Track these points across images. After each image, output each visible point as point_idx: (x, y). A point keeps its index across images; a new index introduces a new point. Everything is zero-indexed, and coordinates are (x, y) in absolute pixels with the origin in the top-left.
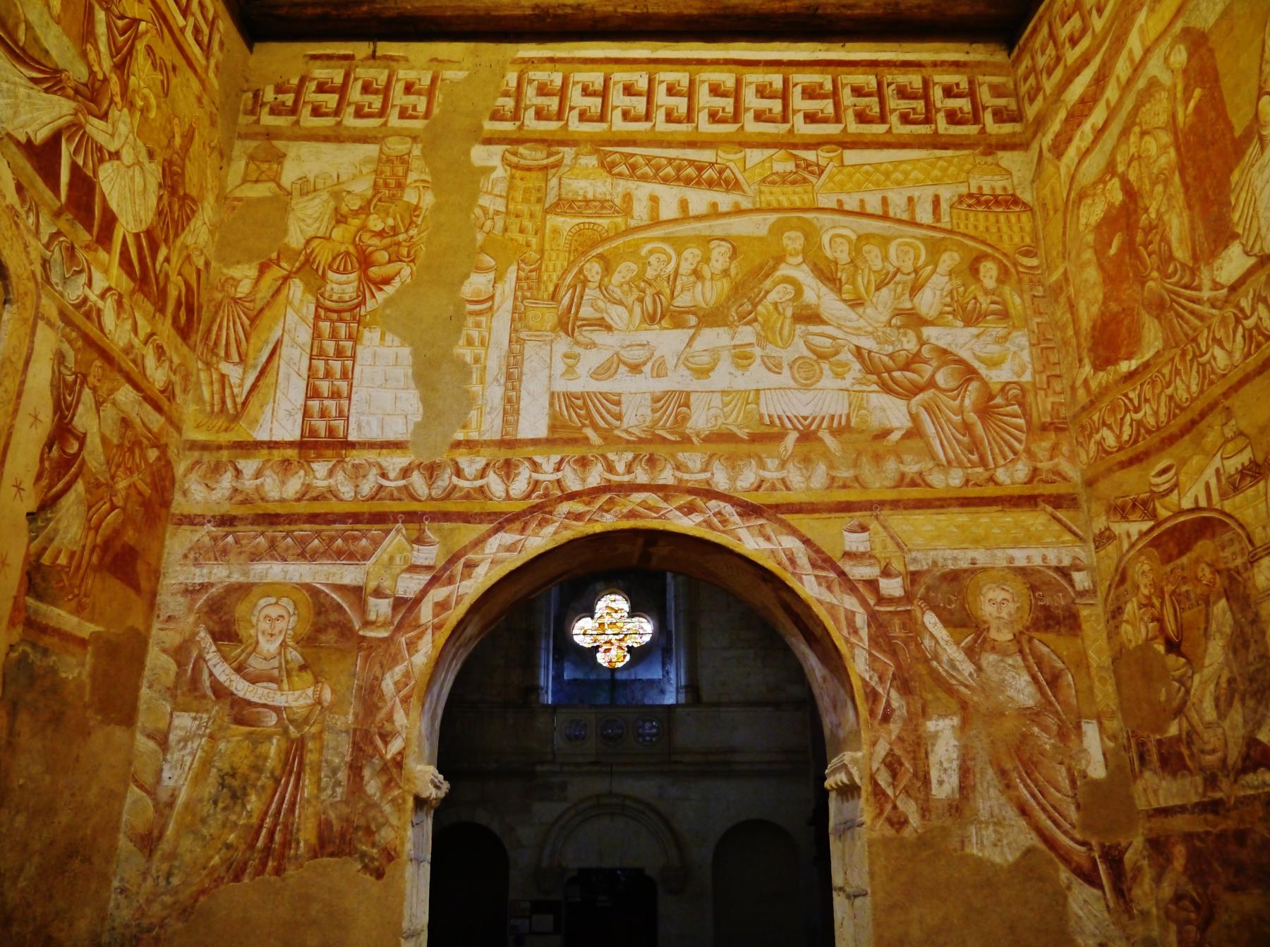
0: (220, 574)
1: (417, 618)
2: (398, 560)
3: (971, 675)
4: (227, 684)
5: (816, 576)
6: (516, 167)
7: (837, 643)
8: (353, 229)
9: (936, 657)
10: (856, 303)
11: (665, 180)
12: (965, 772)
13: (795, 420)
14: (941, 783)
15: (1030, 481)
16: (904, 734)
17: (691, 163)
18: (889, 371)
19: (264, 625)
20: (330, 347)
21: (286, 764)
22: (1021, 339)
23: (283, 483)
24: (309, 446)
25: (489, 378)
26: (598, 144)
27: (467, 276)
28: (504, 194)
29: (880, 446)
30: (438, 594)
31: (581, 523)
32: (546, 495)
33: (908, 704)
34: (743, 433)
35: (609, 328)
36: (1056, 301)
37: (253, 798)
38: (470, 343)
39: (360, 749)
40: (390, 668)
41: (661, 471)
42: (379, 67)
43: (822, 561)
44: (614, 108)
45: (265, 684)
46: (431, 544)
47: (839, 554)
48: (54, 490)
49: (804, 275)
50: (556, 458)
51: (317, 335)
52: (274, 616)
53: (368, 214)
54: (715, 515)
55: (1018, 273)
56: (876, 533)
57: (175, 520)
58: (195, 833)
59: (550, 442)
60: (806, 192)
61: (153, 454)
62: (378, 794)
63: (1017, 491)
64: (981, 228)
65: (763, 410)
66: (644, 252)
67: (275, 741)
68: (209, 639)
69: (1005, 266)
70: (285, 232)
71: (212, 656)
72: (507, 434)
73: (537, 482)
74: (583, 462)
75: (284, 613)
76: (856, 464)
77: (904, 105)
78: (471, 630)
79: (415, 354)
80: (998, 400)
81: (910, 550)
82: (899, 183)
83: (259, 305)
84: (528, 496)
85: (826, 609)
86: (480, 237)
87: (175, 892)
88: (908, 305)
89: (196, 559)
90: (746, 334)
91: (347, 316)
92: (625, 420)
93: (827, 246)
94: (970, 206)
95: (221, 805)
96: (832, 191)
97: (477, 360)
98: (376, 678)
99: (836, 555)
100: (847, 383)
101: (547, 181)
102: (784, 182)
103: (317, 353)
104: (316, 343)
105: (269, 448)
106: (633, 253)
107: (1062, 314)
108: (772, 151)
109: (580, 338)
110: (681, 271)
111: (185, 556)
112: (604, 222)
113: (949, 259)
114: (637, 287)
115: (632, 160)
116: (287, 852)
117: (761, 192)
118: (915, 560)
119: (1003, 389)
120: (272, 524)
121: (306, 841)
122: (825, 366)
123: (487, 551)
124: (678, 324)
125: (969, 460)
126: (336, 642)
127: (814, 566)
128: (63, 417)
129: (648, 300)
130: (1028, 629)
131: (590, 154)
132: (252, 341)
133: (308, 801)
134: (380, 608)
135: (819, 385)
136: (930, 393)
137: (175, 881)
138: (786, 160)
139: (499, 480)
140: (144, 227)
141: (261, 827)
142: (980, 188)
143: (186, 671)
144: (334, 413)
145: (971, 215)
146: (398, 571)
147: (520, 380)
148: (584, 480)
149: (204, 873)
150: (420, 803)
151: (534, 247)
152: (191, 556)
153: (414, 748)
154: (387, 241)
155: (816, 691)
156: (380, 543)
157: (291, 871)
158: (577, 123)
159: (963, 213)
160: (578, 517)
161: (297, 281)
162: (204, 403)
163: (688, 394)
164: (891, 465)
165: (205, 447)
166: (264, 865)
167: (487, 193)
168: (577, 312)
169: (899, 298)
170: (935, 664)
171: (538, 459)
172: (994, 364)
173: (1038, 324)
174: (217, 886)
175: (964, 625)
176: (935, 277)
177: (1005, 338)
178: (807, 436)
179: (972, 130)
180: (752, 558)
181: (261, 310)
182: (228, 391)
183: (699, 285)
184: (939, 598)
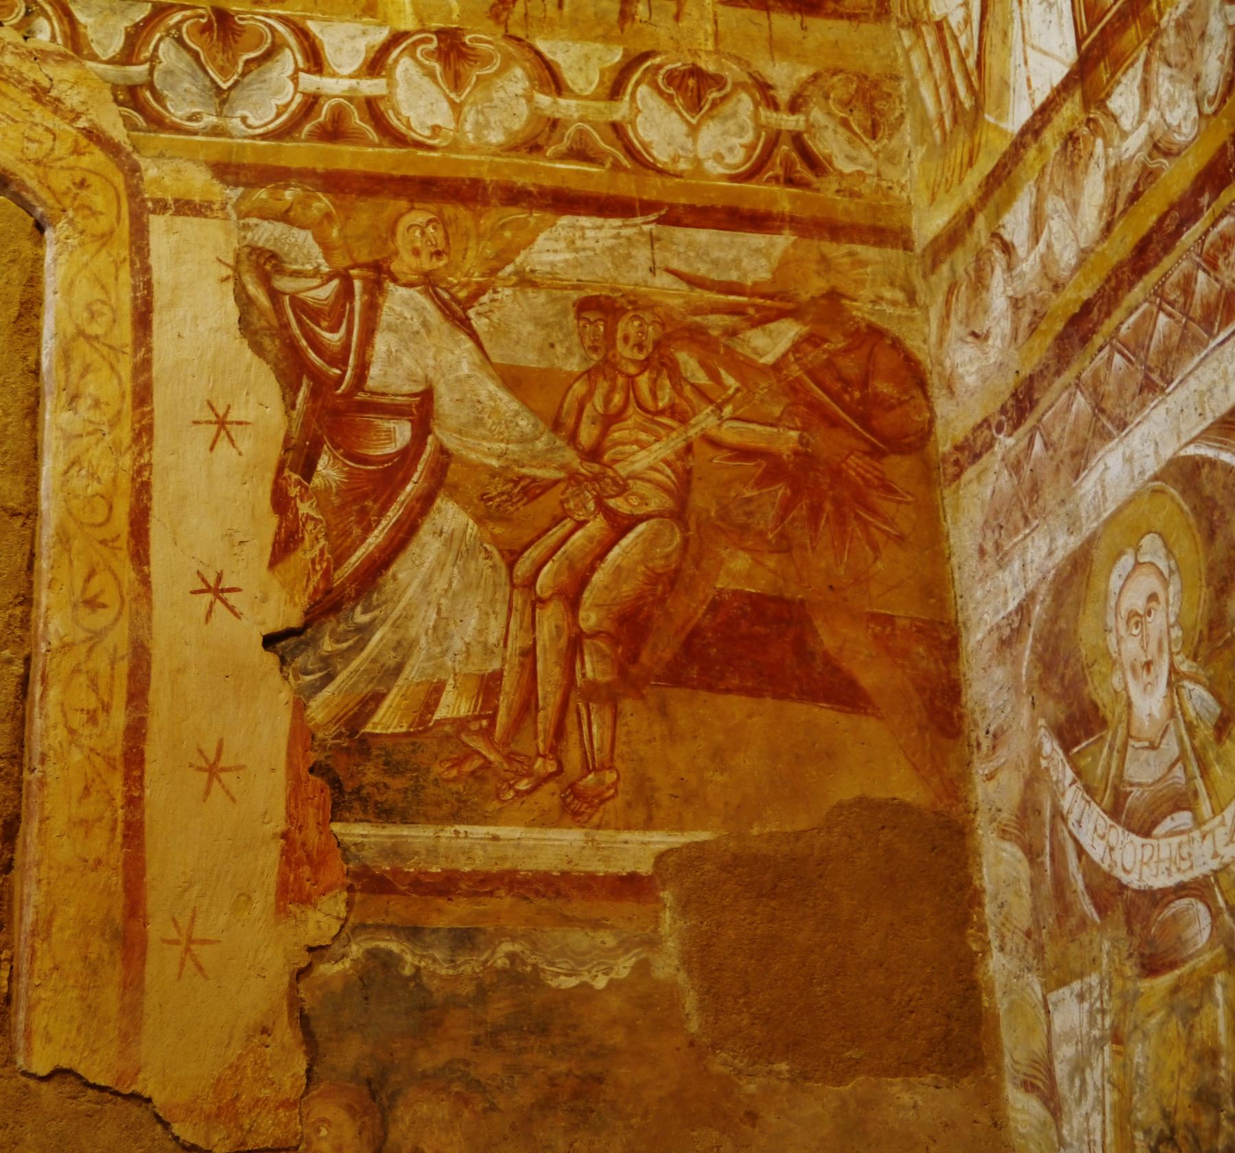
48: (356, 558)
52: (1140, 605)
61: (773, 342)
128: (321, 386)
143: (1043, 863)
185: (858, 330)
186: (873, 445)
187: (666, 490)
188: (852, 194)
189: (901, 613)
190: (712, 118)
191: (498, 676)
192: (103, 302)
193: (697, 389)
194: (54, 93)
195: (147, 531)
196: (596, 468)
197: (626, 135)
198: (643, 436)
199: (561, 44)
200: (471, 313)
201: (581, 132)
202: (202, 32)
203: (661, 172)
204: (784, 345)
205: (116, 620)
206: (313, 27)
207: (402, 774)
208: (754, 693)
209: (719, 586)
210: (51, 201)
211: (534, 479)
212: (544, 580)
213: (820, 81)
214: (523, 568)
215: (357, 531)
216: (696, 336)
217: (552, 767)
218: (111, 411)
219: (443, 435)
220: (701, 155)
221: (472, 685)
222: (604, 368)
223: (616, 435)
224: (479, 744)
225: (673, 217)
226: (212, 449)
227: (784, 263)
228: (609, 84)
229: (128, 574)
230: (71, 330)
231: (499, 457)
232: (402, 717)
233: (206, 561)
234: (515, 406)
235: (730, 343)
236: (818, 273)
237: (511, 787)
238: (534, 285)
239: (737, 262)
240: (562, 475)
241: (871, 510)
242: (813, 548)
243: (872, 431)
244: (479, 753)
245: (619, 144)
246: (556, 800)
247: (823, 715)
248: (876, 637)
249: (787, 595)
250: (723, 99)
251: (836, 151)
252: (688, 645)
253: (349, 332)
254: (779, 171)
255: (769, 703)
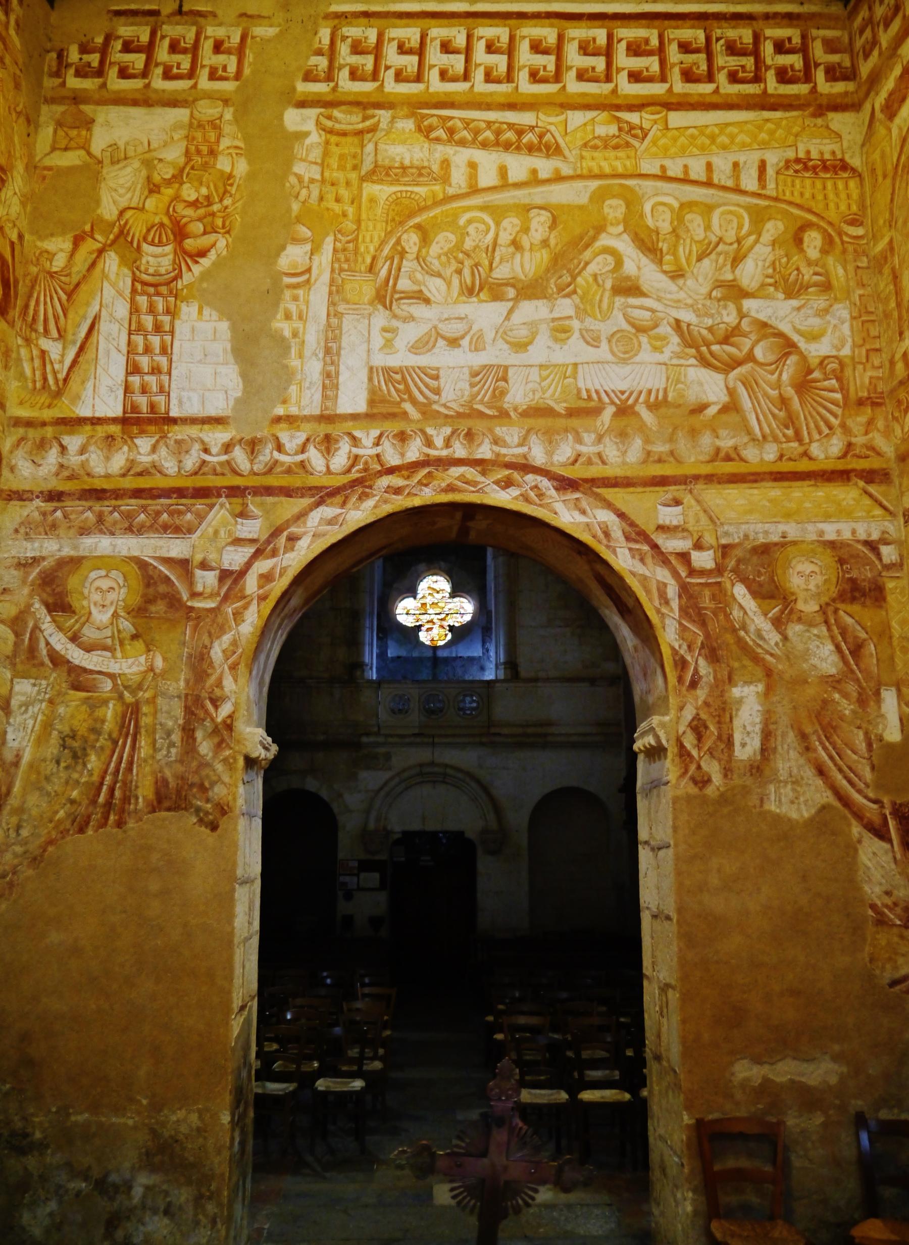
0: (51, 548)
1: (243, 589)
2: (222, 533)
3: (777, 644)
4: (63, 653)
5: (630, 549)
6: (331, 132)
7: (649, 613)
8: (166, 199)
9: (744, 627)
10: (677, 275)
11: (484, 145)
12: (767, 735)
13: (612, 395)
14: (744, 745)
15: (844, 456)
16: (710, 700)
17: (511, 126)
18: (708, 345)
19: (96, 597)
20: (148, 321)
21: (122, 726)
22: (842, 311)
23: (108, 459)
24: (131, 422)
25: (307, 353)
26: (415, 106)
27: (283, 248)
28: (319, 161)
29: (697, 420)
30: (263, 566)
31: (400, 497)
32: (365, 470)
33: (715, 671)
34: (560, 408)
35: (427, 301)
36: (880, 272)
37: (93, 758)
38: (288, 317)
39: (193, 713)
40: (218, 638)
41: (479, 445)
42: (186, 23)
43: (637, 534)
44: (431, 67)
45: (99, 652)
46: (254, 518)
47: (653, 528)
49: (625, 246)
50: (375, 433)
51: (134, 309)
52: (105, 587)
53: (182, 183)
54: (531, 489)
55: (843, 242)
56: (692, 507)
57: (4, 496)
58: (40, 789)
59: (369, 417)
60: (628, 157)
62: (211, 754)
63: (830, 465)
64: (807, 195)
65: (581, 385)
66: (462, 221)
67: (111, 705)
68: (44, 611)
69: (830, 236)
70: (98, 202)
71: (47, 625)
72: (326, 409)
73: (356, 457)
74: (402, 437)
75: (115, 586)
76: (671, 440)
77: (733, 62)
78: (295, 602)
79: (234, 328)
80: (816, 375)
81: (722, 524)
82: (724, 148)
83: (75, 279)
84: (349, 471)
85: (639, 581)
86: (295, 207)
87: (25, 843)
88: (730, 277)
89: (27, 534)
90: (565, 307)
91: (164, 290)
92: (443, 394)
93: (649, 215)
94: (796, 171)
95: (63, 765)
96: (655, 156)
97: (295, 335)
98: (206, 647)
99: (650, 528)
100: (665, 357)
101: (362, 146)
102: (606, 147)
103: (135, 329)
104: (134, 318)
105: (93, 424)
106: (452, 223)
107: (884, 285)
108: (594, 114)
109: (397, 311)
110: (500, 241)
111: (17, 531)
112: (422, 190)
113: (773, 229)
114: (455, 258)
115: (450, 124)
116: (127, 806)
117: (582, 158)
118: (726, 534)
119: (821, 363)
120: (99, 499)
121: (144, 797)
122: (644, 339)
123: (310, 523)
124: (497, 297)
125: (784, 435)
126: (165, 612)
127: (628, 539)
129: (467, 272)
130: (834, 600)
131: (407, 117)
132: (71, 315)
133: (145, 761)
134: (207, 580)
135: (637, 359)
136: (748, 366)
137: (25, 833)
138: (609, 123)
139: (319, 455)
141: (102, 784)
142: (808, 152)
143: (23, 640)
144: (154, 389)
145: (798, 182)
146: (223, 544)
147: (338, 354)
148: (403, 455)
149: (51, 825)
150: (250, 762)
151: (351, 216)
152: (22, 530)
153: (243, 712)
154: (201, 212)
155: (628, 660)
156: (205, 517)
157: (131, 824)
158: (393, 83)
159: (789, 179)
160: (398, 491)
161: (112, 254)
162: (26, 379)
163: (506, 368)
164: (706, 441)
165: (29, 423)
166: (106, 818)
167: (301, 160)
168: (395, 284)
169: (720, 269)
170: (742, 633)
171: (357, 434)
172: (814, 337)
173: (860, 296)
174: (63, 838)
175: (772, 597)
176: (758, 247)
177: (826, 311)
178: (624, 411)
179: (802, 89)
180: (568, 531)
181: (78, 285)
182: (49, 368)
183: (518, 256)
184: (749, 570)
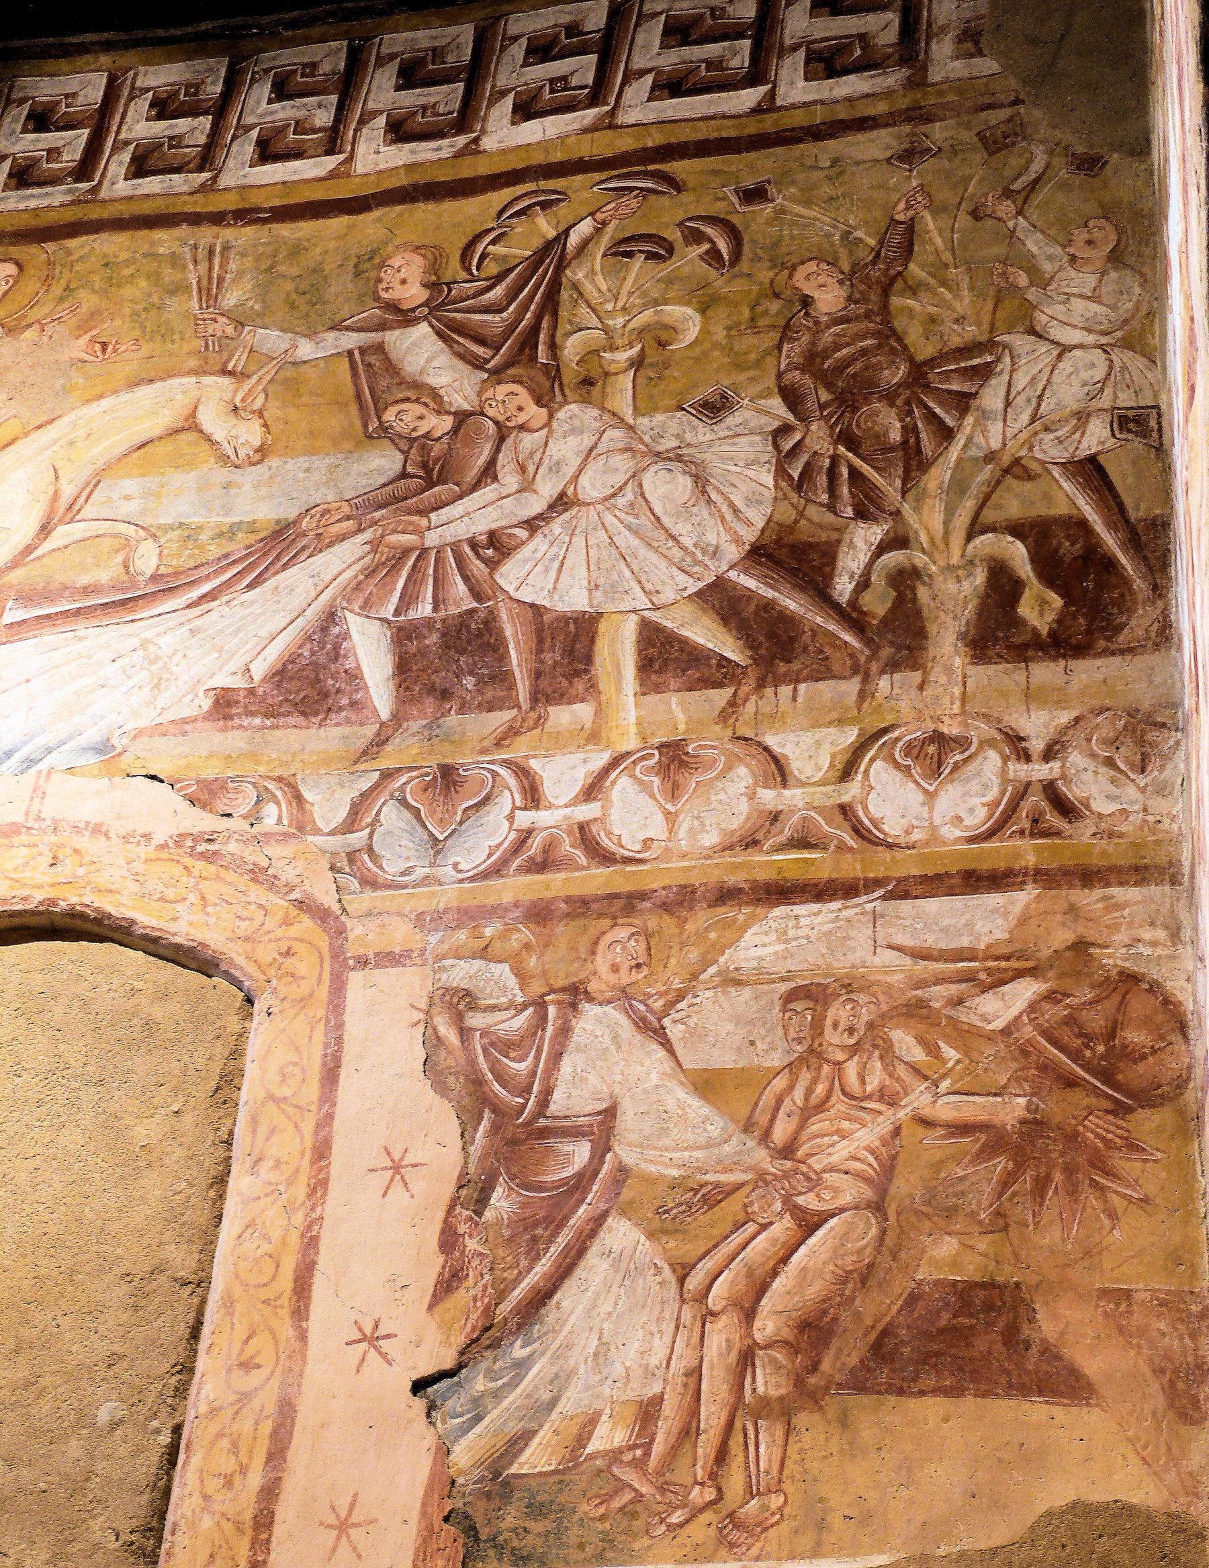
140: (733, 553)
185: (1108, 978)
186: (1117, 1101)
187: (868, 1180)
188: (1111, 835)
189: (1141, 1286)
190: (952, 781)
191: (658, 1400)
192: (295, 1064)
193: (916, 1070)
194: (270, 872)
195: (310, 1285)
196: (788, 1164)
197: (855, 816)
198: (845, 1125)
199: (791, 737)
200: (666, 1022)
201: (804, 819)
202: (425, 790)
203: (890, 846)
204: (1019, 1005)
205: (268, 1379)
206: (534, 764)
207: (545, 1516)
208: (955, 1392)
209: (920, 1277)
210: (257, 974)
211: (717, 1185)
212: (718, 1294)
213: (1082, 723)
214: (694, 1282)
215: (524, 1263)
216: (915, 1011)
217: (710, 1494)
218: (288, 1170)
219: (624, 1152)
220: (937, 822)
221: (631, 1412)
222: (812, 1056)
223: (815, 1127)
224: (629, 1476)
225: (903, 891)
226: (384, 1195)
227: (1023, 920)
228: (840, 766)
229: (287, 1330)
230: (262, 1095)
231: (679, 1167)
232: (553, 1452)
233: (364, 1310)
234: (706, 1110)
235: (952, 1013)
236: (1064, 924)
237: (662, 1521)
238: (738, 983)
239: (970, 926)
240: (749, 1176)
241: (1110, 1174)
242: (1036, 1224)
243: (1116, 1087)
244: (630, 1486)
245: (846, 825)
246: (712, 1532)
247: (1037, 1410)
248: (1106, 1315)
249: (999, 1279)
250: (965, 761)
251: (1095, 793)
252: (877, 1347)
253: (537, 1058)
254: (1026, 824)
255: (969, 1403)
